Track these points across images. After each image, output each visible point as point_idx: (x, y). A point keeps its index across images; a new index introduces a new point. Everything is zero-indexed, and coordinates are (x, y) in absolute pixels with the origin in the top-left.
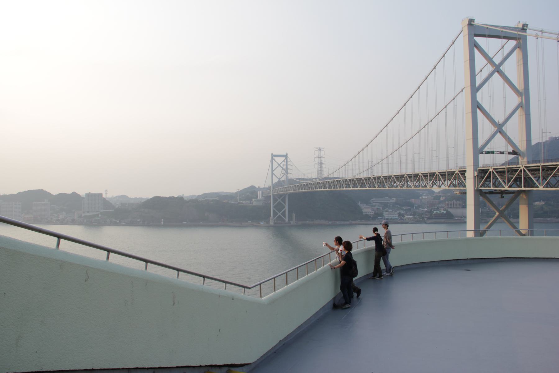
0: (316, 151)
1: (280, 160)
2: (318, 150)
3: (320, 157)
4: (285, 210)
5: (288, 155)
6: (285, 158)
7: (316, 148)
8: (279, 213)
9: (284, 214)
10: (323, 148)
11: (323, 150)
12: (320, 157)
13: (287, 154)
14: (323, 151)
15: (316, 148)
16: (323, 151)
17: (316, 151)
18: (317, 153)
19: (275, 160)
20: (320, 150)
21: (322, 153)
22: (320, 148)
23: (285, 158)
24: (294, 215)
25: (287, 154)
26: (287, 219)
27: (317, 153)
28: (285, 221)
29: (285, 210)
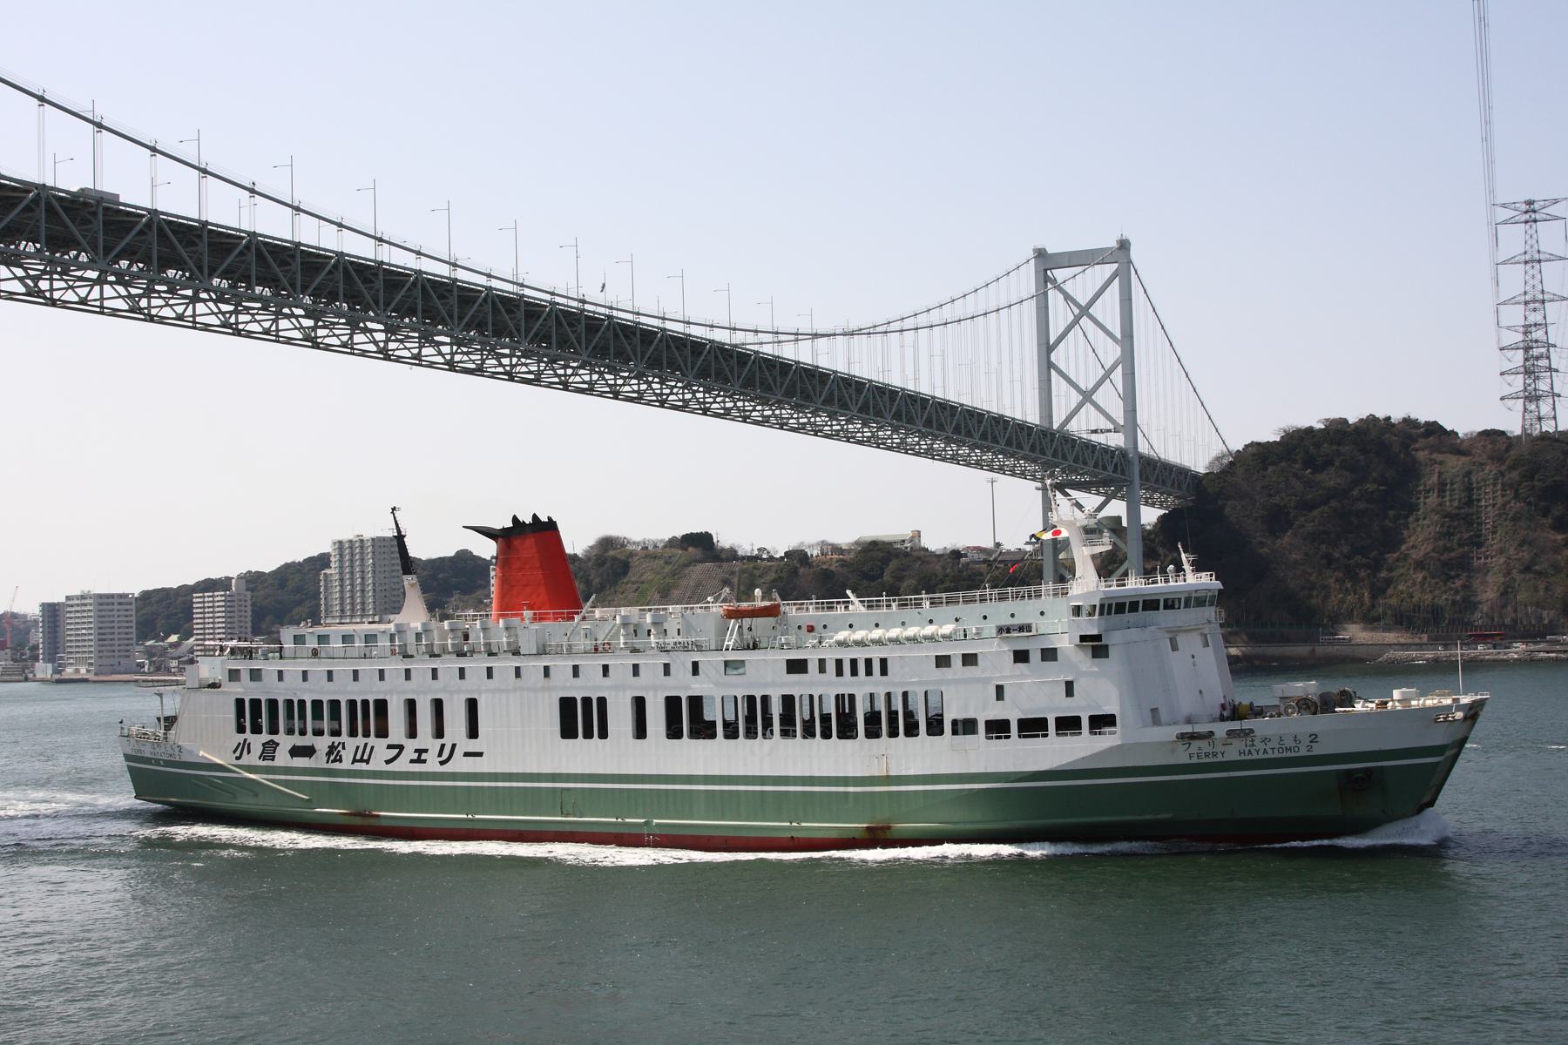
0: (1505, 222)
1: (1082, 284)
5: (1135, 254)
6: (1110, 269)
10: (1556, 201)
11: (1552, 210)
13: (1124, 245)
14: (1557, 218)
16: (1557, 218)
17: (1505, 222)
18: (1514, 239)
19: (1058, 288)
21: (1549, 237)
22: (1529, 203)
23: (1110, 269)
25: (1124, 245)
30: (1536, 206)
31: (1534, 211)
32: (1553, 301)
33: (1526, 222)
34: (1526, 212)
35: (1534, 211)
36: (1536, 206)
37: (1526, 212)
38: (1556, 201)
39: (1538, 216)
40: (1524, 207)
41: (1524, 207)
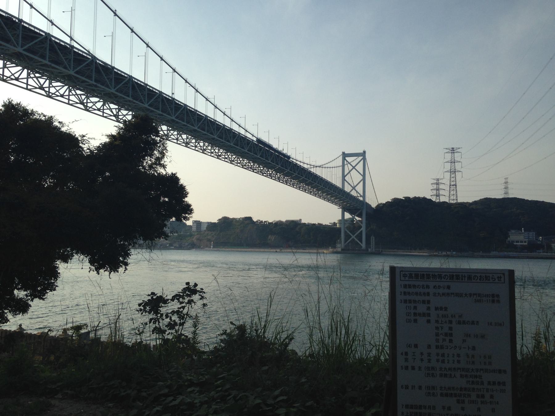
0: (446, 153)
2: (451, 152)
3: (453, 162)
4: (362, 231)
7: (446, 149)
8: (354, 238)
9: (360, 237)
10: (459, 148)
12: (453, 162)
14: (459, 152)
15: (446, 149)
16: (459, 152)
17: (446, 153)
18: (449, 157)
20: (453, 151)
21: (457, 156)
22: (453, 148)
24: (373, 239)
26: (363, 245)
27: (449, 157)
28: (362, 247)
29: (362, 232)
30: (454, 149)
31: (454, 150)
32: (457, 172)
33: (452, 153)
34: (452, 150)
35: (454, 150)
36: (454, 149)
37: (452, 150)
38: (459, 148)
39: (455, 152)
40: (451, 149)
41: (451, 149)
